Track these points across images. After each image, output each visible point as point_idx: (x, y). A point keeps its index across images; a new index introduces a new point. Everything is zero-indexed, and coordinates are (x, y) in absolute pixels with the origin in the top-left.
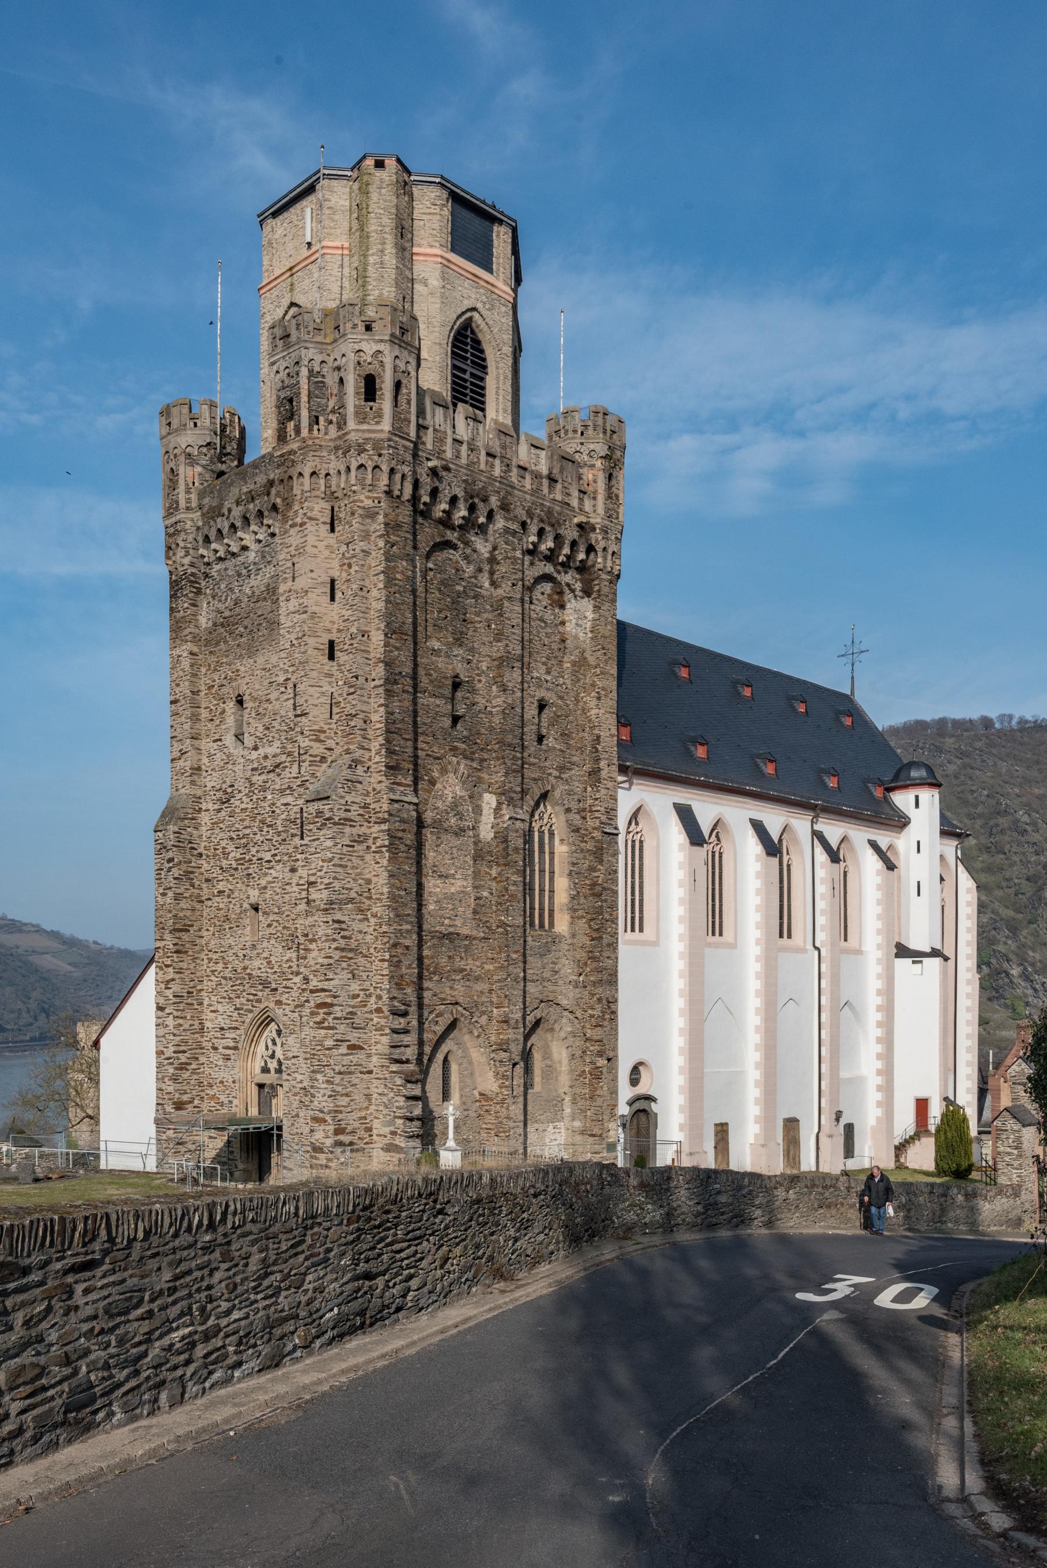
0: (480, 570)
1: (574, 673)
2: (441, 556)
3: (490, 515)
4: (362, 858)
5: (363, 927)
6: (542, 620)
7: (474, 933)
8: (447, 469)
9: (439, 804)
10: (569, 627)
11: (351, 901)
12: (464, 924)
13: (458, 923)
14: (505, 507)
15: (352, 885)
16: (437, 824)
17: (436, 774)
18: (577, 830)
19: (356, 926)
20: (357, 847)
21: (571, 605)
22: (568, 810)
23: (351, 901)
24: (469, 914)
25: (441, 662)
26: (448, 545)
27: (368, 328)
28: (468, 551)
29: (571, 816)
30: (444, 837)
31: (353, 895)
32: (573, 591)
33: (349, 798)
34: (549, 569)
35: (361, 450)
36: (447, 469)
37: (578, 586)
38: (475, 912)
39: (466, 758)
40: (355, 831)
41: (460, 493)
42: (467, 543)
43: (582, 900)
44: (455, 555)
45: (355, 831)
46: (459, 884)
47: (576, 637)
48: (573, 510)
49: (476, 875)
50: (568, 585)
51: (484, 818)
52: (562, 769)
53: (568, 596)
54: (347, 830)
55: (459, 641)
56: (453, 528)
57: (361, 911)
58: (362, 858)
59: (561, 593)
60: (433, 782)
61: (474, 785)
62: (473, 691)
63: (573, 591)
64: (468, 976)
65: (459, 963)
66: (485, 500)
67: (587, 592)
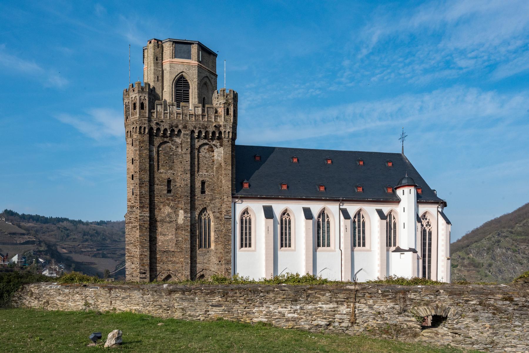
0: (178, 147)
1: (217, 171)
2: (164, 146)
3: (180, 131)
4: (135, 232)
5: (136, 250)
6: (204, 157)
7: (176, 250)
8: (162, 122)
9: (163, 215)
10: (215, 158)
11: (132, 243)
12: (172, 248)
13: (170, 247)
14: (185, 127)
15: (132, 239)
16: (162, 221)
17: (161, 207)
18: (218, 218)
19: (133, 250)
20: (134, 229)
21: (216, 150)
22: (214, 212)
23: (132, 243)
24: (174, 245)
25: (163, 176)
26: (166, 142)
27: (134, 91)
28: (173, 142)
29: (215, 214)
30: (164, 224)
31: (132, 242)
32: (216, 146)
33: (131, 216)
34: (206, 141)
35: (133, 123)
36: (162, 122)
37: (218, 144)
38: (176, 244)
39: (172, 201)
40: (133, 225)
41: (167, 127)
42: (172, 141)
43: (220, 239)
44: (169, 144)
45: (133, 225)
46: (170, 236)
47: (217, 160)
48: (213, 122)
49: (176, 234)
50: (214, 145)
51: (179, 218)
52: (211, 200)
53: (214, 148)
54: (130, 225)
55: (171, 169)
56: (167, 137)
57: (135, 246)
58: (135, 232)
59: (212, 147)
60: (160, 209)
61: (175, 209)
62: (175, 182)
63: (216, 146)
64: (173, 262)
65: (170, 259)
66: (177, 126)
67: (221, 145)
